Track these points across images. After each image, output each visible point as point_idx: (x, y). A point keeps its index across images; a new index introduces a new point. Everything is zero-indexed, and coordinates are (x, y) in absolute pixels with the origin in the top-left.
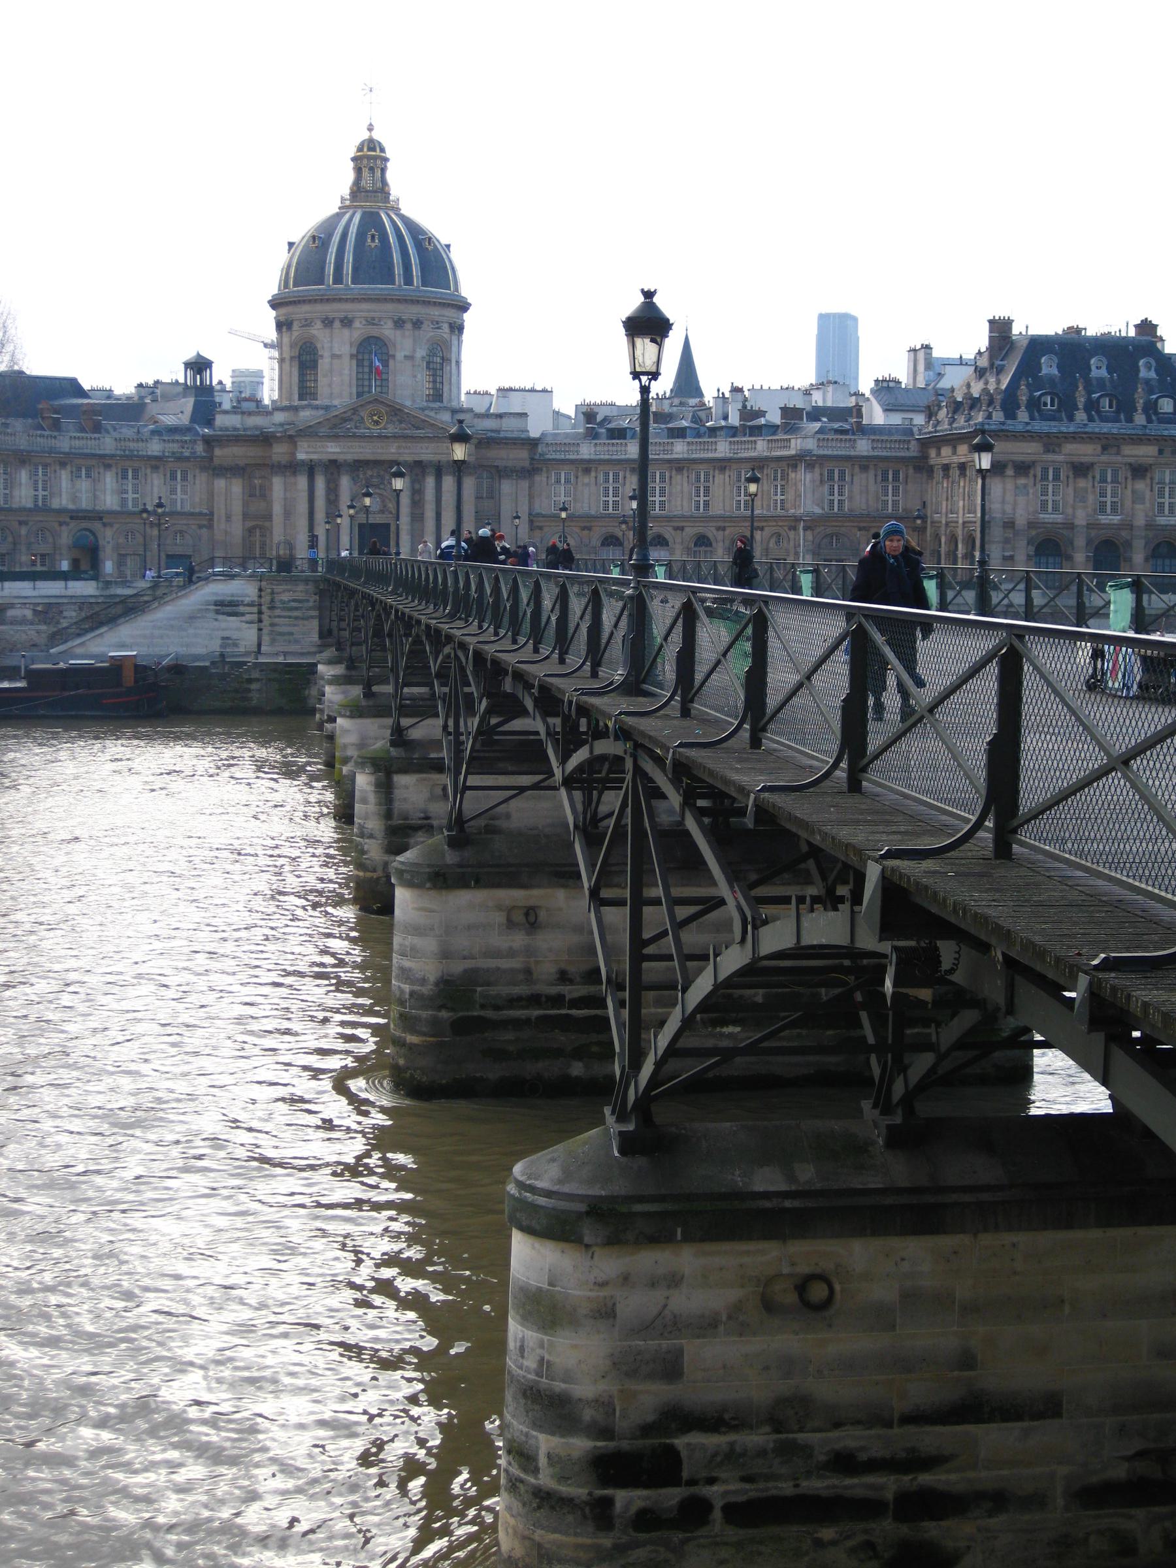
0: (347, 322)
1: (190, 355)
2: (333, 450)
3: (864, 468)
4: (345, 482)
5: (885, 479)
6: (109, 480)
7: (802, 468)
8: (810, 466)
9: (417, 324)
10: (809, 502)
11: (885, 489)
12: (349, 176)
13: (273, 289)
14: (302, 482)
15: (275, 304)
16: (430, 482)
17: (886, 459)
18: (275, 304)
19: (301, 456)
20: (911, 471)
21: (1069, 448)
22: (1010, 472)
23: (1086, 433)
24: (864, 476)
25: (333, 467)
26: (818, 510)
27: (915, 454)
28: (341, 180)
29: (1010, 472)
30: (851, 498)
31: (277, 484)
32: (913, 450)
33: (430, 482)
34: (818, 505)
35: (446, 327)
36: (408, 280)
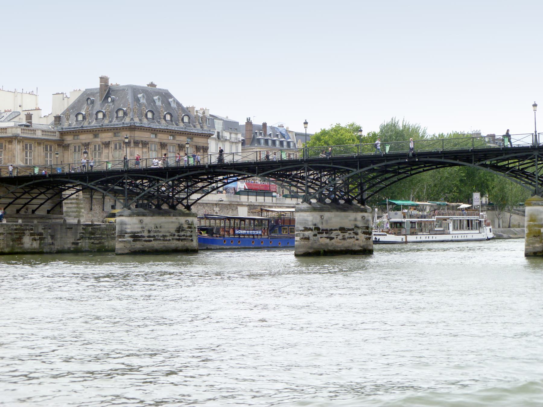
3: (39, 144)
5: (47, 150)
7: (15, 142)
8: (19, 142)
10: (19, 160)
11: (46, 154)
17: (47, 140)
20: (56, 146)
21: (160, 136)
22: (140, 146)
23: (167, 129)
24: (39, 147)
26: (22, 164)
27: (58, 138)
29: (140, 146)
30: (34, 158)
32: (57, 137)
34: (22, 161)
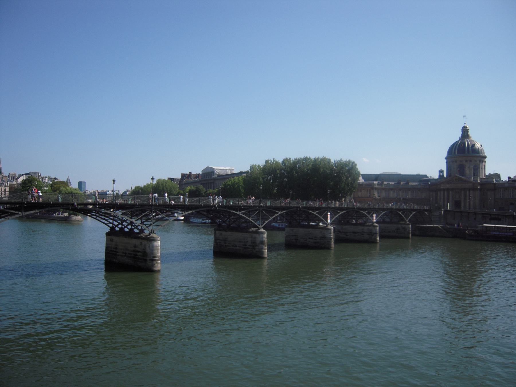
0: (456, 161)
1: (439, 169)
2: (448, 186)
4: (450, 192)
6: (410, 193)
9: (471, 161)
12: (461, 133)
13: (446, 156)
14: (442, 192)
15: (446, 158)
16: (468, 192)
18: (446, 158)
19: (442, 187)
25: (448, 190)
28: (459, 134)
31: (439, 193)
33: (468, 192)
35: (478, 161)
36: (469, 152)
